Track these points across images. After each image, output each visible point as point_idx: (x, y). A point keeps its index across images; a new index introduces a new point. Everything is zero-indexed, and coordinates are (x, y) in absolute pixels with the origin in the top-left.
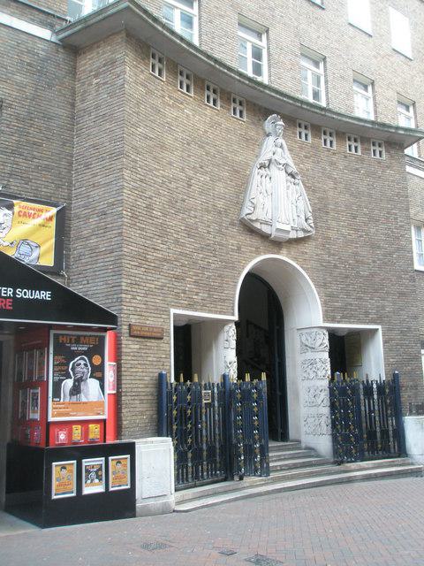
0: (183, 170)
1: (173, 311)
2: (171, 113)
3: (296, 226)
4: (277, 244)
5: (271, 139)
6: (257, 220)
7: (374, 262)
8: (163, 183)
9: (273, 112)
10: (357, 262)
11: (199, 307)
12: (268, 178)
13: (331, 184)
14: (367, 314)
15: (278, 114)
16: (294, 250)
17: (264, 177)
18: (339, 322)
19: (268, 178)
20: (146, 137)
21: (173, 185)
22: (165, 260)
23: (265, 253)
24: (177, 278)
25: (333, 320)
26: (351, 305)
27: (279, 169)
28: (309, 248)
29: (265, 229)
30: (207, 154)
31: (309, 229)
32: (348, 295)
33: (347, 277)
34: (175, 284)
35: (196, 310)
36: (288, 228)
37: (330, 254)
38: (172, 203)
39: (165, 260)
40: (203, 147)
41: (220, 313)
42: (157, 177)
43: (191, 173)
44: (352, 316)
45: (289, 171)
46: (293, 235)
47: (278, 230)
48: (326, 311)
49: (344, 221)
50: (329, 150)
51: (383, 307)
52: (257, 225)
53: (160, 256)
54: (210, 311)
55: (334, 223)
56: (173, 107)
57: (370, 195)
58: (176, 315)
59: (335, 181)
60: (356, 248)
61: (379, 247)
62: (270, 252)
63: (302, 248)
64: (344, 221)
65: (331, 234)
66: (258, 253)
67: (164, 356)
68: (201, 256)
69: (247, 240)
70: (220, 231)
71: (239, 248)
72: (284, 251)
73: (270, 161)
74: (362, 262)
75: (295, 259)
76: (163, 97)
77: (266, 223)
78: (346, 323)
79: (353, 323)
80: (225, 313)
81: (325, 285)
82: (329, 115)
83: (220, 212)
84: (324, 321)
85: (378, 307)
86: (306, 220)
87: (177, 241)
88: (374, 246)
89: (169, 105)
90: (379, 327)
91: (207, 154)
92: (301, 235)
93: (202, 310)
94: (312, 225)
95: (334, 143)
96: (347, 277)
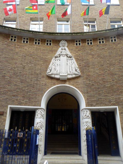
0: (21, 64)
1: (9, 106)
2: (17, 50)
3: (71, 73)
4: (64, 81)
5: (60, 48)
6: (52, 74)
7: (113, 80)
8: (11, 69)
9: (61, 40)
10: (104, 82)
11: (23, 104)
12: (59, 60)
13: (91, 56)
14: (110, 102)
15: (64, 40)
16: (72, 82)
17: (57, 60)
18: (94, 106)
19: (59, 60)
20: (5, 57)
21: (16, 69)
22: (9, 91)
23: (58, 84)
24: (14, 96)
25: (92, 106)
26: (101, 99)
27: (63, 56)
28: (80, 81)
29: (57, 77)
30: (33, 58)
31: (78, 73)
32: (99, 94)
33: (99, 88)
34: (12, 97)
35: (22, 105)
36: (66, 74)
37: (90, 81)
38: (14, 74)
39: (9, 91)
40: (31, 57)
41: (34, 106)
42: (9, 67)
43: (25, 65)
44: (102, 103)
45: (68, 56)
46: (70, 77)
47: (61, 76)
48: (88, 102)
49: (97, 68)
50: (90, 46)
51: (119, 98)
52: (53, 76)
53: (6, 90)
54: (29, 106)
55: (92, 70)
56: (19, 48)
57: (110, 56)
58: (10, 107)
59: (93, 55)
60: (103, 76)
61: (116, 74)
62: (60, 84)
63: (76, 81)
64: (97, 68)
65: (91, 74)
66: (55, 85)
67: (3, 121)
68: (27, 88)
69: (50, 81)
70: (37, 80)
71: (45, 84)
72: (67, 83)
73: (60, 55)
74: (107, 82)
75: (73, 85)
76: (15, 46)
77: (57, 74)
78: (98, 106)
79: (101, 106)
80: (36, 106)
81: (87, 92)
82: (85, 34)
83: (38, 74)
84: (86, 106)
85: (116, 98)
86: (76, 70)
87: (16, 85)
88: (112, 74)
89: (18, 48)
90: (117, 107)
91: (33, 58)
92: (74, 76)
93: (25, 105)
94: (79, 72)
95: (92, 43)
96: (99, 88)
